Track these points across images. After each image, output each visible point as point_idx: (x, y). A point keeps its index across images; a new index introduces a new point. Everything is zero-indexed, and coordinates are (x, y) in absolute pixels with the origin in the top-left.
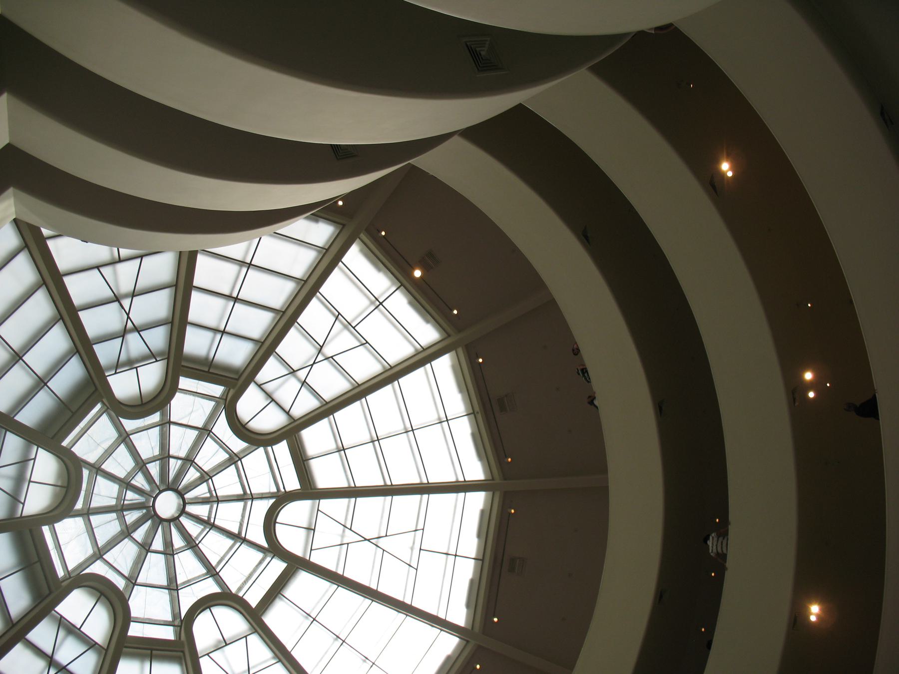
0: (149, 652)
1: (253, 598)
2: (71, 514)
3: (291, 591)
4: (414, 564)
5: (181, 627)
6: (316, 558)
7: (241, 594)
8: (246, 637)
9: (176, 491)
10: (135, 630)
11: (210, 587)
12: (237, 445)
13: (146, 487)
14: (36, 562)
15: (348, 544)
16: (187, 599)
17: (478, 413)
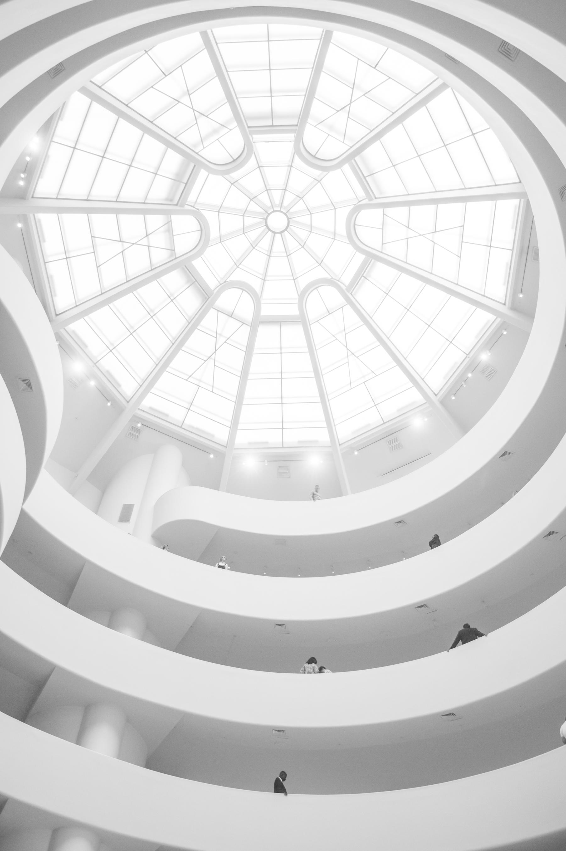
0: (194, 280)
1: (266, 311)
2: (224, 176)
3: (288, 330)
4: (353, 386)
5: (221, 284)
6: (315, 329)
7: (262, 302)
8: (244, 323)
9: (288, 219)
10: (197, 264)
11: (256, 284)
12: (342, 230)
13: (277, 201)
14: (183, 183)
15: (337, 339)
16: (238, 276)
17: (469, 357)
